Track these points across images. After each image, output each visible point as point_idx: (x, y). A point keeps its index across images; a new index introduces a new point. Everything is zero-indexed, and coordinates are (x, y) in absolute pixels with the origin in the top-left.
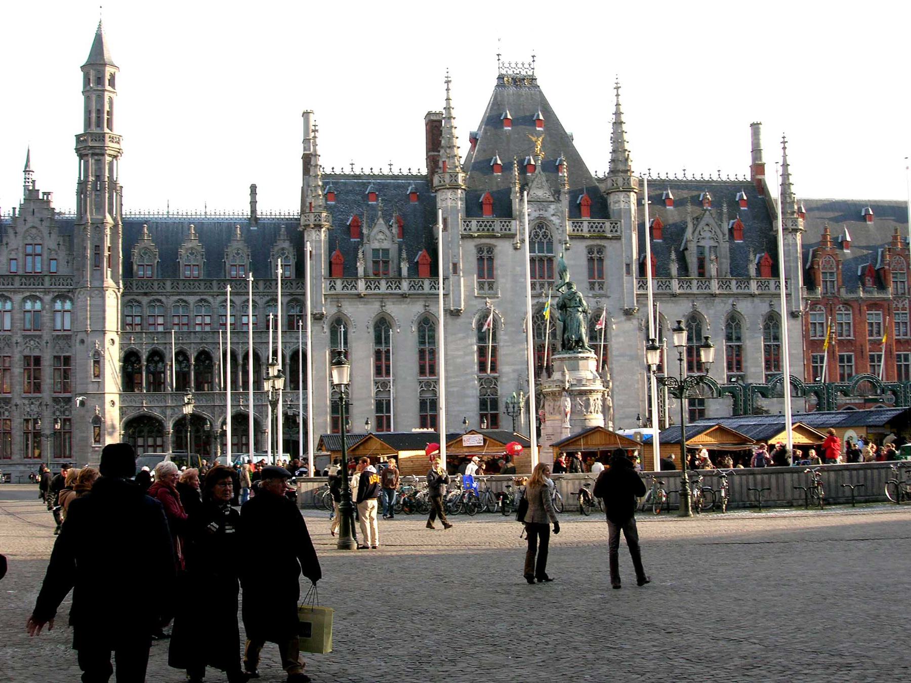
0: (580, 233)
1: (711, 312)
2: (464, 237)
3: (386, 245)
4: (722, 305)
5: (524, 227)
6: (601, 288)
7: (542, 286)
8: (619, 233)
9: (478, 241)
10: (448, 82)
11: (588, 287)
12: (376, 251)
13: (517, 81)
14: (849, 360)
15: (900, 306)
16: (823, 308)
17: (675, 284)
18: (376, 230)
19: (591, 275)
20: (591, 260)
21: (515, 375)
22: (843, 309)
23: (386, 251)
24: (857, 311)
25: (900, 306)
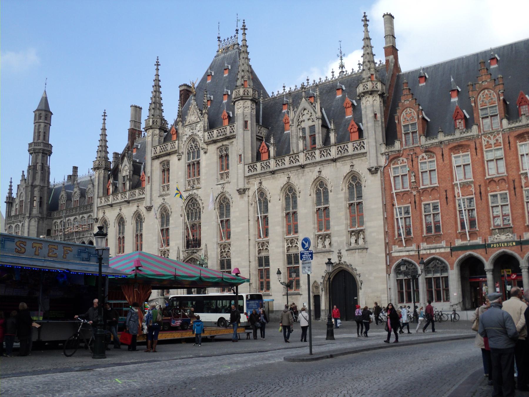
1: (302, 181)
2: (153, 159)
4: (310, 173)
6: (227, 177)
7: (194, 181)
8: (234, 133)
11: (219, 177)
12: (124, 177)
14: (435, 208)
15: (492, 142)
16: (405, 160)
17: (273, 165)
20: (221, 157)
22: (426, 157)
23: (127, 176)
24: (440, 157)
25: (492, 142)
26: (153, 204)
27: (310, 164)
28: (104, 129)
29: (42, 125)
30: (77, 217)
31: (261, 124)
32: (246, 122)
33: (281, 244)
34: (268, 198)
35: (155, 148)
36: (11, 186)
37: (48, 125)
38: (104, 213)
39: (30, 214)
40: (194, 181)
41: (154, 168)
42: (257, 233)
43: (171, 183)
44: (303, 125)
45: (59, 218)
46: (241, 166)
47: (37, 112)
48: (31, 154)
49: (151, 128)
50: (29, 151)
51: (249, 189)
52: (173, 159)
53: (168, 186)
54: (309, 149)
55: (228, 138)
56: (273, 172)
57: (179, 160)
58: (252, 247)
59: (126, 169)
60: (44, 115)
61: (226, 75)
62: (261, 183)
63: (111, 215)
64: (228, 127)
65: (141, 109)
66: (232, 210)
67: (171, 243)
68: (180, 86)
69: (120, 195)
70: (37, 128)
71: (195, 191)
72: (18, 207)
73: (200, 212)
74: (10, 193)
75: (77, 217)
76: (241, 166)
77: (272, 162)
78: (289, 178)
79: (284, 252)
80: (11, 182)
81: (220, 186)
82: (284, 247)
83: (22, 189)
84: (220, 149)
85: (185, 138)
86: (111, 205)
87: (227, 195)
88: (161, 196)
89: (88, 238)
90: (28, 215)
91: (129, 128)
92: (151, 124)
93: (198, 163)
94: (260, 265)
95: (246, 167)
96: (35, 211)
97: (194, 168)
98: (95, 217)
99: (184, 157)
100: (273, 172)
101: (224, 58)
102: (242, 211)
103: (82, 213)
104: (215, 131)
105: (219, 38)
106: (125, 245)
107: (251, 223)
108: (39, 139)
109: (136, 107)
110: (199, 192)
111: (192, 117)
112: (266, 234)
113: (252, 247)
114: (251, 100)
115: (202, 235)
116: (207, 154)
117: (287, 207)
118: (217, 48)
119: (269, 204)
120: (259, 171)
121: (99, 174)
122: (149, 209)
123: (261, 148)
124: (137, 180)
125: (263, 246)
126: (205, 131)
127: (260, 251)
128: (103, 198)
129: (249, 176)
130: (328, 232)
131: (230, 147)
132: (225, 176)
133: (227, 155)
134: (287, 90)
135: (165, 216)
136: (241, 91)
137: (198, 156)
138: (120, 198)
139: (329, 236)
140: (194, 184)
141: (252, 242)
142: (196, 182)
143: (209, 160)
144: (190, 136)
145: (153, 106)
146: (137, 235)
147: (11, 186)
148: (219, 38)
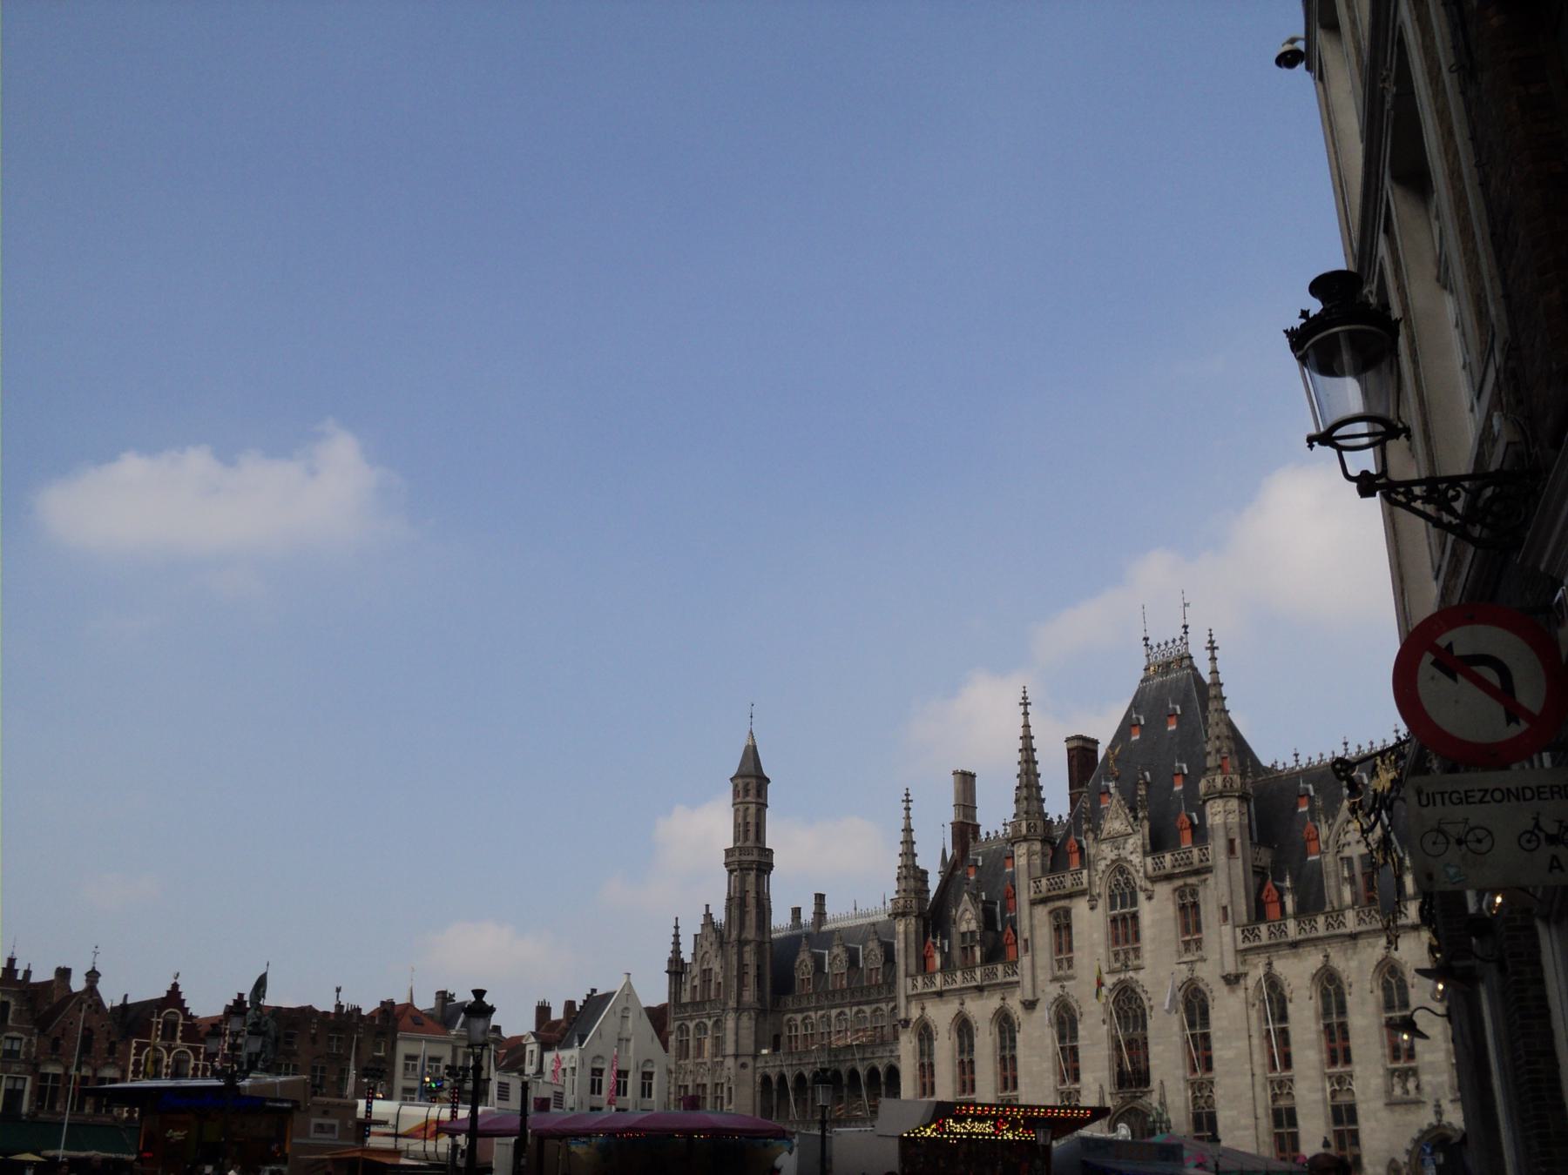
0: (1162, 872)
1: (1354, 964)
2: (1033, 903)
3: (973, 926)
5: (1098, 878)
6: (1199, 948)
7: (1126, 953)
9: (1051, 906)
10: (1026, 704)
11: (1182, 948)
12: (964, 934)
13: (1166, 667)
18: (961, 909)
19: (1186, 930)
20: (1183, 908)
21: (1096, 1087)
23: (973, 933)
26: (1039, 994)
27: (1368, 932)
28: (908, 830)
29: (753, 809)
30: (847, 1010)
31: (1256, 839)
32: (1231, 842)
33: (1319, 1085)
34: (1287, 993)
35: (1037, 880)
36: (677, 936)
37: (762, 806)
38: (923, 1009)
39: (738, 1002)
40: (1126, 953)
41: (1036, 922)
42: (1266, 1061)
43: (1077, 955)
44: (1347, 852)
45: (801, 1011)
46: (1227, 929)
47: (740, 782)
48: (731, 872)
49: (1025, 839)
50: (726, 865)
51: (1246, 975)
52: (1080, 907)
53: (1070, 961)
54: (1363, 900)
55: (1197, 872)
56: (1295, 945)
57: (1092, 908)
58: (1258, 1089)
59: (967, 919)
60: (752, 785)
61: (1172, 727)
62: (1270, 964)
63: (941, 1015)
64: (1195, 851)
65: (973, 776)
66: (1213, 1014)
67: (1084, 1076)
68: (1068, 740)
69: (959, 973)
70: (741, 814)
71: (1131, 974)
72: (697, 982)
73: (1144, 1015)
74: (676, 951)
75: (847, 1010)
76: (1227, 929)
77: (1291, 925)
78: (1327, 956)
79: (1325, 1100)
80: (677, 927)
81: (1183, 967)
82: (1324, 1090)
83: (706, 944)
84: (1180, 892)
85: (1102, 865)
86: (940, 994)
87: (1201, 985)
88: (1055, 979)
89: (886, 1061)
90: (732, 1003)
91: (952, 819)
92: (1024, 830)
93: (1135, 916)
94: (1278, 1122)
95: (1238, 931)
96: (749, 995)
97: (1125, 929)
98: (902, 1015)
99: (1102, 904)
100: (1295, 945)
101: (1162, 685)
102: (1233, 1019)
103: (859, 1004)
104: (1168, 857)
105: (1146, 639)
106: (978, 1077)
107: (1256, 1041)
108: (746, 839)
109: (964, 774)
110: (1141, 976)
111: (1115, 823)
112: (1287, 1062)
113: (1258, 1089)
114: (1239, 797)
115: (1152, 1063)
116: (1154, 901)
117: (1326, 1012)
118: (1144, 663)
119: (1291, 1008)
120: (1265, 940)
121: (906, 926)
122: (1030, 1005)
123: (1265, 893)
124: (997, 943)
125: (1281, 1088)
126: (1145, 854)
127: (1275, 1097)
128: (920, 979)
129: (1246, 950)
130: (1413, 1064)
131: (1201, 890)
132: (1193, 947)
133: (1195, 905)
134: (1303, 762)
135: (1066, 1021)
136: (1219, 780)
137: (1134, 903)
138: (959, 980)
139: (1414, 1072)
140: (1127, 958)
141: (1259, 1079)
142: (1132, 956)
143: (1156, 913)
144: (1113, 862)
145: (1025, 792)
146: (1003, 1059)
147: (677, 936)
148: (1146, 639)
